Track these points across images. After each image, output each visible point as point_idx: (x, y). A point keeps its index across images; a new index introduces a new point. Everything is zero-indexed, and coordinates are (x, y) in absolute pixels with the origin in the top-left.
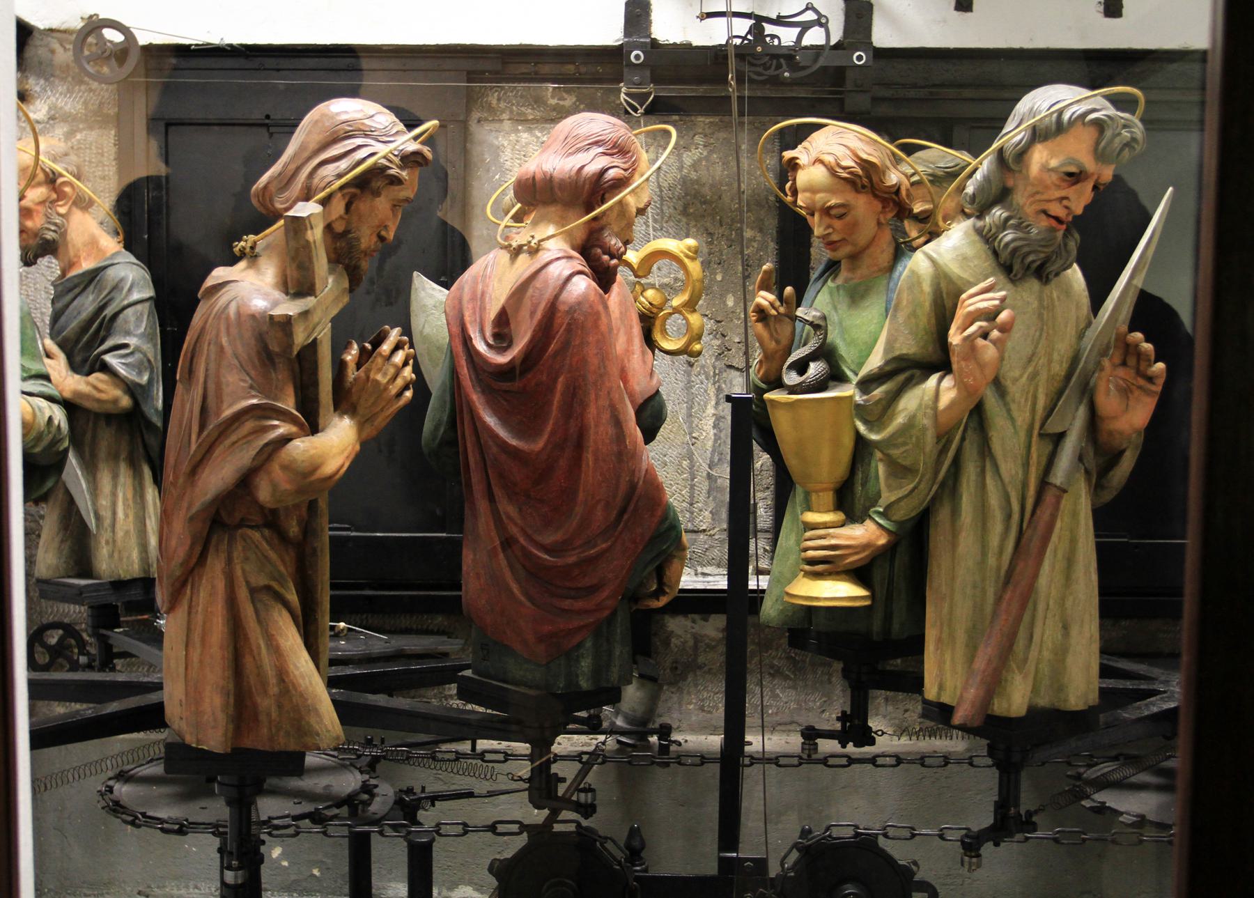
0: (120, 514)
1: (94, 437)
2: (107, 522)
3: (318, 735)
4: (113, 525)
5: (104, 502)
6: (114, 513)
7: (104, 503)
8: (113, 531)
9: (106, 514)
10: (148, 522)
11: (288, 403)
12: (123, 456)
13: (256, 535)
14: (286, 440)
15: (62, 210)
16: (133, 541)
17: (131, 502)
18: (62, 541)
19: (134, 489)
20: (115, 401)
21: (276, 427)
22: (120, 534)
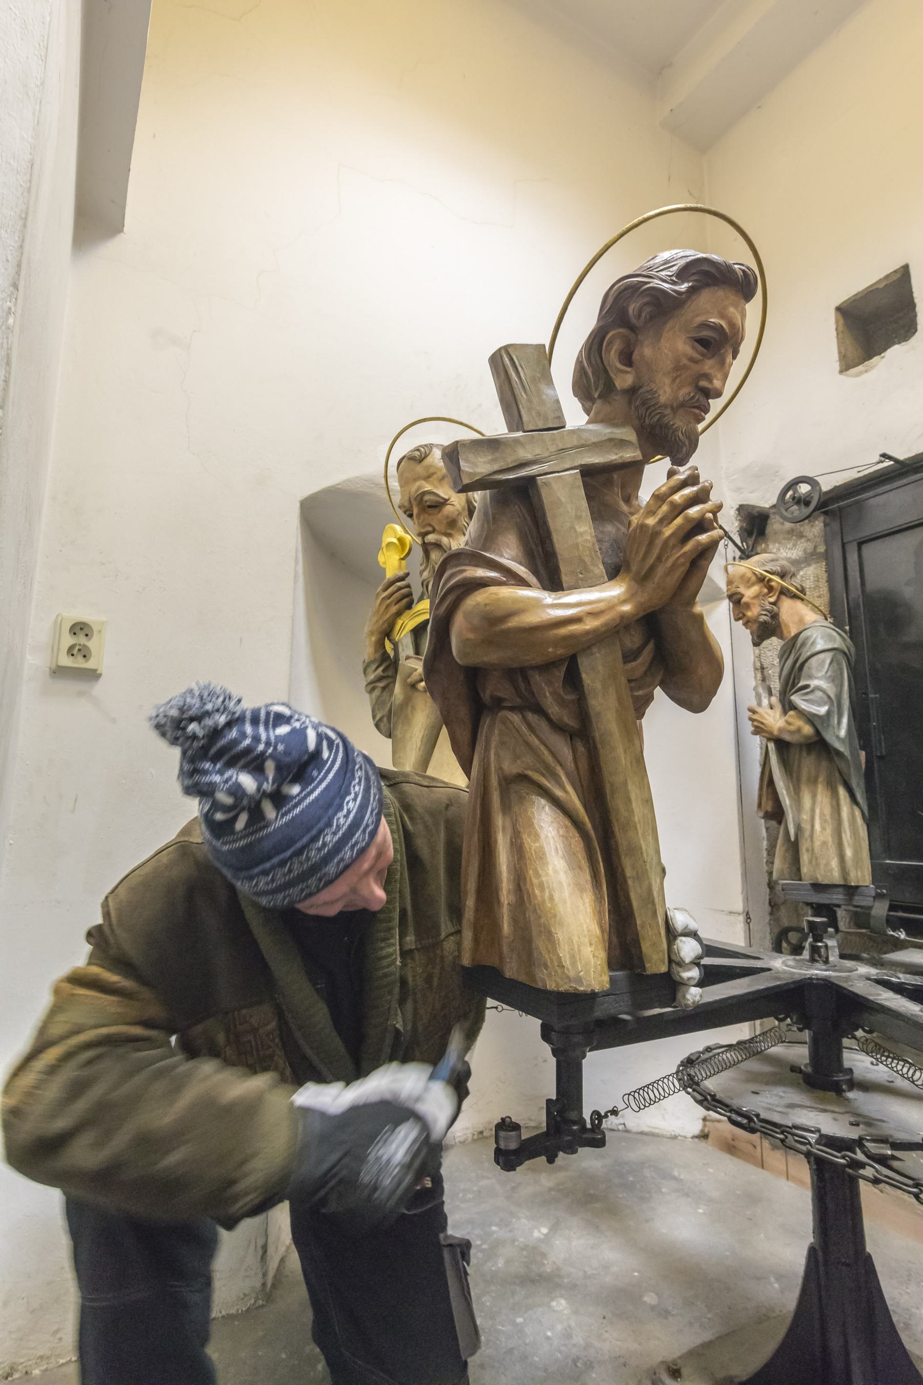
0: (818, 827)
1: (799, 766)
2: (807, 833)
3: (546, 967)
4: (812, 836)
5: (805, 817)
6: (813, 826)
7: (805, 817)
8: (812, 841)
9: (806, 826)
10: (843, 836)
11: (509, 554)
12: (820, 779)
13: (515, 718)
14: (482, 584)
16: (832, 851)
17: (828, 818)
18: (787, 850)
19: (832, 807)
20: (799, 730)
21: (464, 571)
22: (817, 844)
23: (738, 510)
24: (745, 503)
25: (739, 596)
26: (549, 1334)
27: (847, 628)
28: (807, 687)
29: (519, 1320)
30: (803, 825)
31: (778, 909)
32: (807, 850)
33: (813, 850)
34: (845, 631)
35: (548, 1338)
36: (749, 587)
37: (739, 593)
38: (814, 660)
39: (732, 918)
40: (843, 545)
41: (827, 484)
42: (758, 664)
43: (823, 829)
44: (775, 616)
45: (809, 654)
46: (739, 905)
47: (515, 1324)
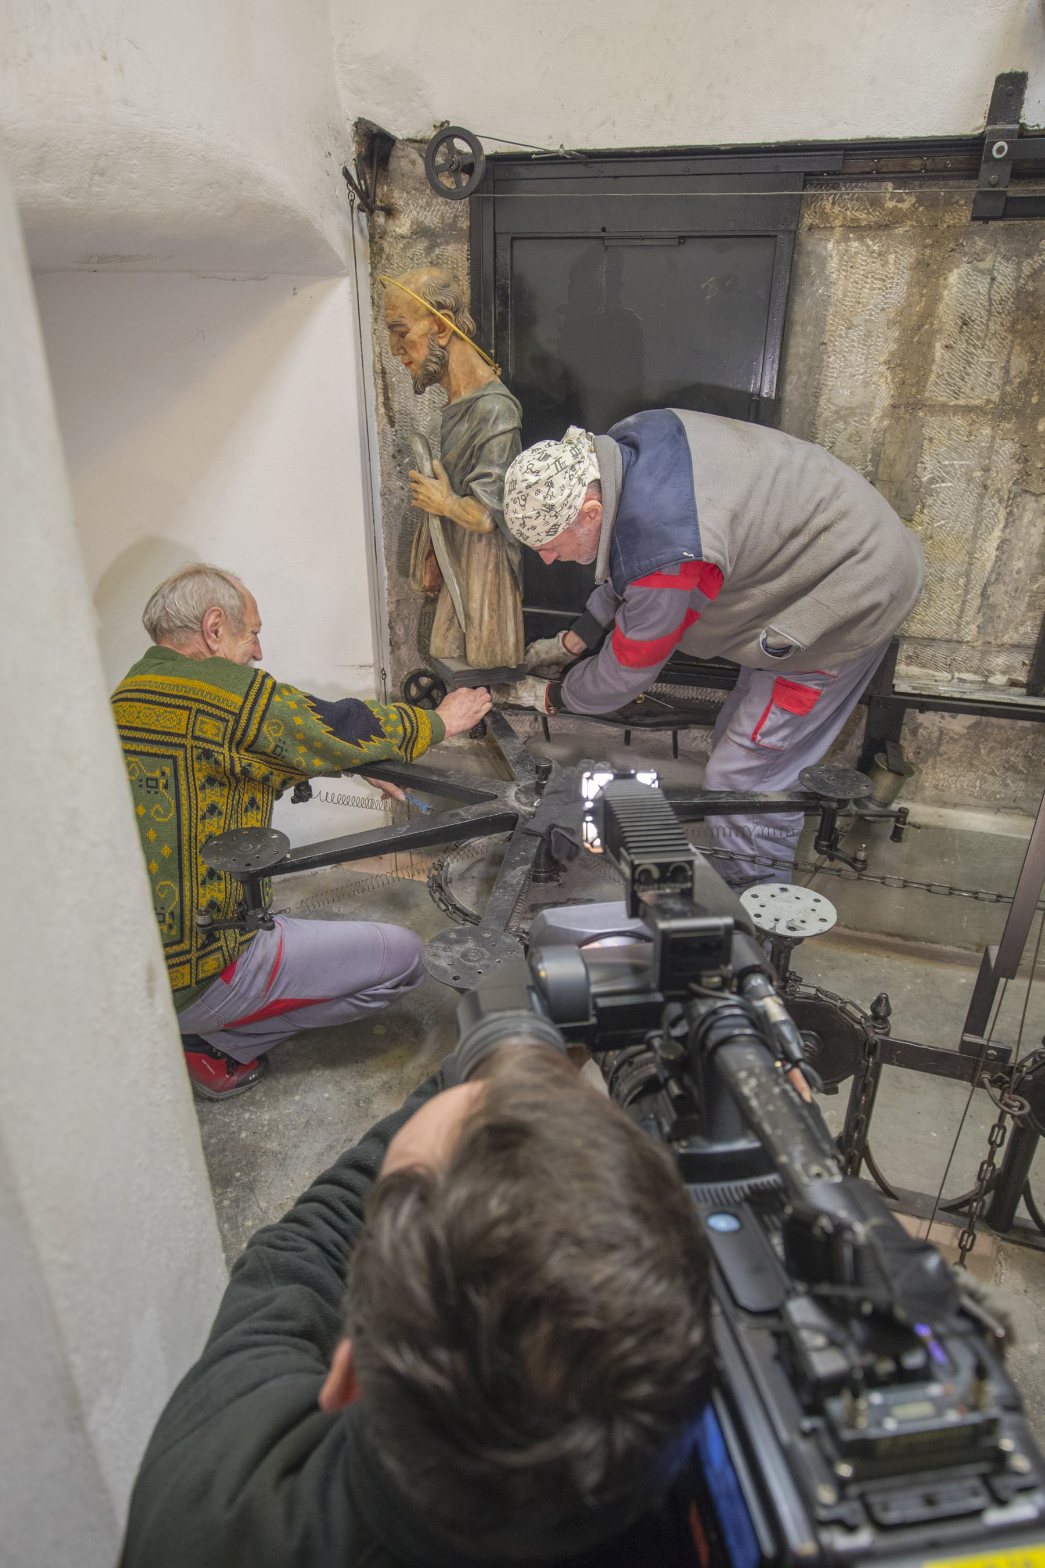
15: (443, 342)
23: (356, 124)
24: (367, 118)
25: (403, 329)
26: (326, 1095)
27: (493, 351)
28: (488, 475)
29: (297, 1098)
30: (473, 614)
31: (399, 649)
32: (476, 638)
33: (481, 638)
34: (490, 355)
35: (328, 1099)
36: (416, 320)
37: (404, 325)
38: (495, 441)
39: (363, 671)
40: (495, 234)
41: (489, 148)
42: (378, 367)
43: (491, 618)
44: (444, 363)
45: (491, 434)
46: (369, 658)
47: (296, 1103)
